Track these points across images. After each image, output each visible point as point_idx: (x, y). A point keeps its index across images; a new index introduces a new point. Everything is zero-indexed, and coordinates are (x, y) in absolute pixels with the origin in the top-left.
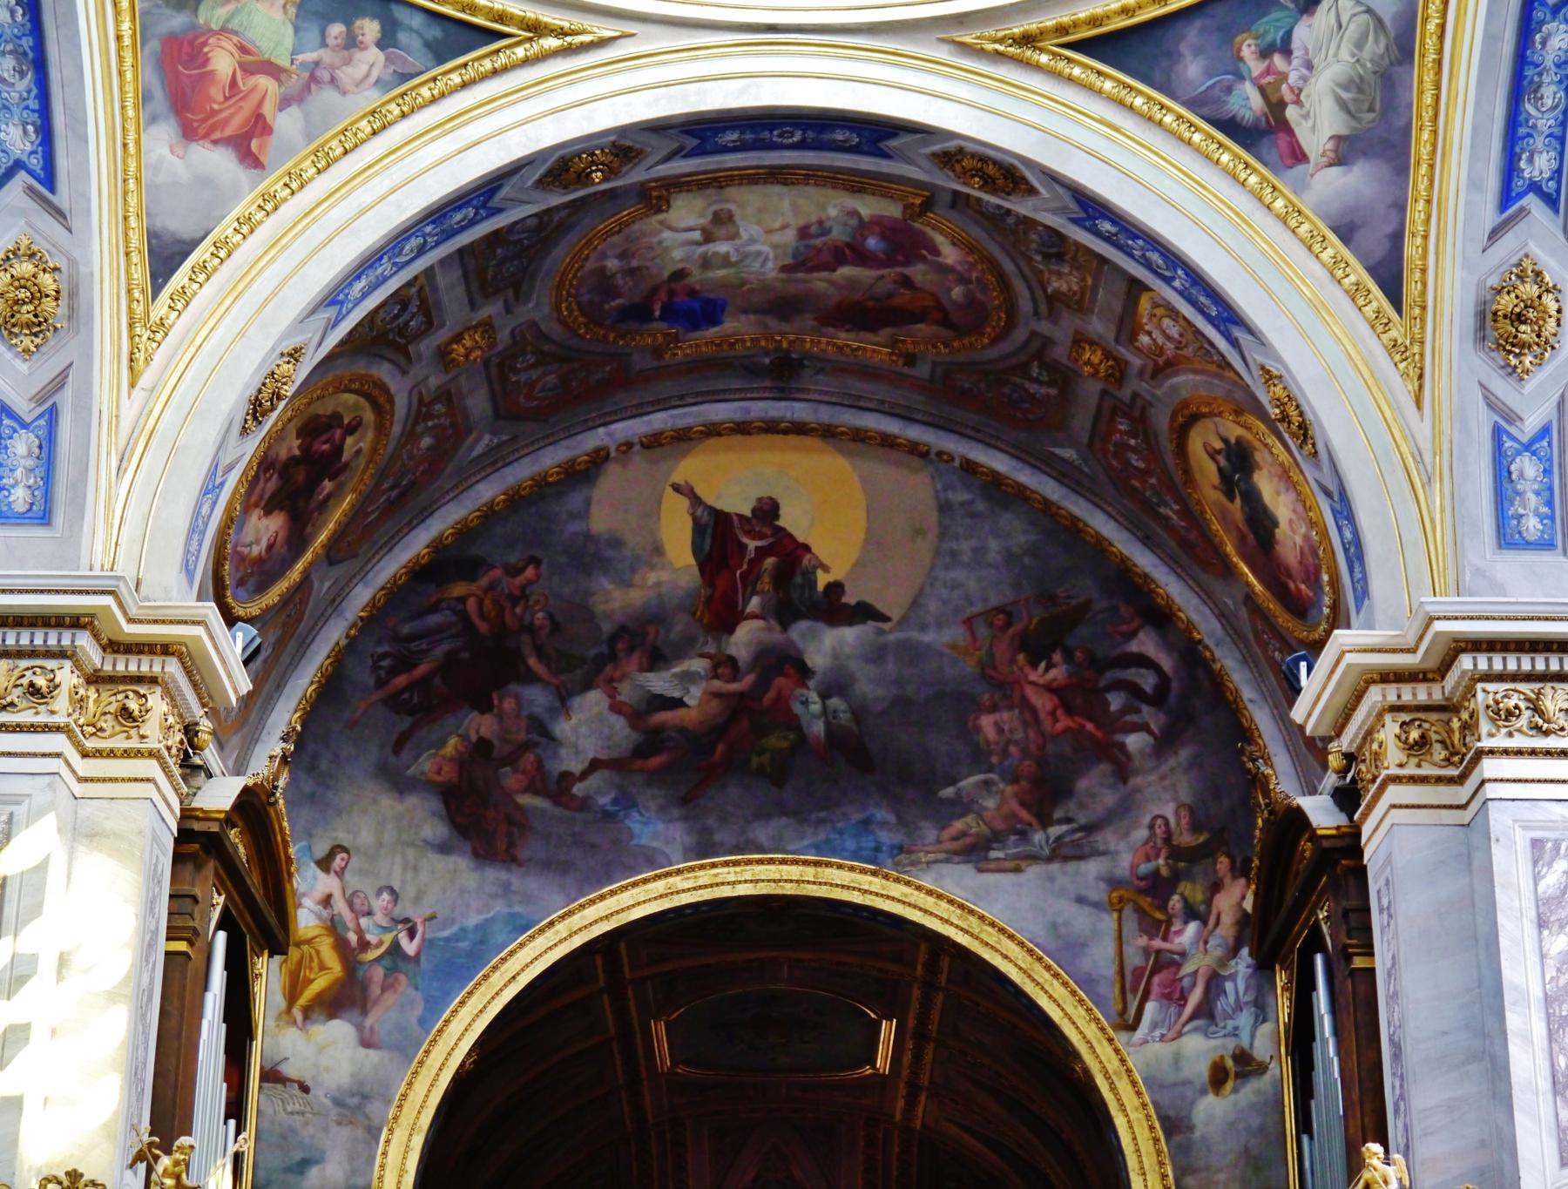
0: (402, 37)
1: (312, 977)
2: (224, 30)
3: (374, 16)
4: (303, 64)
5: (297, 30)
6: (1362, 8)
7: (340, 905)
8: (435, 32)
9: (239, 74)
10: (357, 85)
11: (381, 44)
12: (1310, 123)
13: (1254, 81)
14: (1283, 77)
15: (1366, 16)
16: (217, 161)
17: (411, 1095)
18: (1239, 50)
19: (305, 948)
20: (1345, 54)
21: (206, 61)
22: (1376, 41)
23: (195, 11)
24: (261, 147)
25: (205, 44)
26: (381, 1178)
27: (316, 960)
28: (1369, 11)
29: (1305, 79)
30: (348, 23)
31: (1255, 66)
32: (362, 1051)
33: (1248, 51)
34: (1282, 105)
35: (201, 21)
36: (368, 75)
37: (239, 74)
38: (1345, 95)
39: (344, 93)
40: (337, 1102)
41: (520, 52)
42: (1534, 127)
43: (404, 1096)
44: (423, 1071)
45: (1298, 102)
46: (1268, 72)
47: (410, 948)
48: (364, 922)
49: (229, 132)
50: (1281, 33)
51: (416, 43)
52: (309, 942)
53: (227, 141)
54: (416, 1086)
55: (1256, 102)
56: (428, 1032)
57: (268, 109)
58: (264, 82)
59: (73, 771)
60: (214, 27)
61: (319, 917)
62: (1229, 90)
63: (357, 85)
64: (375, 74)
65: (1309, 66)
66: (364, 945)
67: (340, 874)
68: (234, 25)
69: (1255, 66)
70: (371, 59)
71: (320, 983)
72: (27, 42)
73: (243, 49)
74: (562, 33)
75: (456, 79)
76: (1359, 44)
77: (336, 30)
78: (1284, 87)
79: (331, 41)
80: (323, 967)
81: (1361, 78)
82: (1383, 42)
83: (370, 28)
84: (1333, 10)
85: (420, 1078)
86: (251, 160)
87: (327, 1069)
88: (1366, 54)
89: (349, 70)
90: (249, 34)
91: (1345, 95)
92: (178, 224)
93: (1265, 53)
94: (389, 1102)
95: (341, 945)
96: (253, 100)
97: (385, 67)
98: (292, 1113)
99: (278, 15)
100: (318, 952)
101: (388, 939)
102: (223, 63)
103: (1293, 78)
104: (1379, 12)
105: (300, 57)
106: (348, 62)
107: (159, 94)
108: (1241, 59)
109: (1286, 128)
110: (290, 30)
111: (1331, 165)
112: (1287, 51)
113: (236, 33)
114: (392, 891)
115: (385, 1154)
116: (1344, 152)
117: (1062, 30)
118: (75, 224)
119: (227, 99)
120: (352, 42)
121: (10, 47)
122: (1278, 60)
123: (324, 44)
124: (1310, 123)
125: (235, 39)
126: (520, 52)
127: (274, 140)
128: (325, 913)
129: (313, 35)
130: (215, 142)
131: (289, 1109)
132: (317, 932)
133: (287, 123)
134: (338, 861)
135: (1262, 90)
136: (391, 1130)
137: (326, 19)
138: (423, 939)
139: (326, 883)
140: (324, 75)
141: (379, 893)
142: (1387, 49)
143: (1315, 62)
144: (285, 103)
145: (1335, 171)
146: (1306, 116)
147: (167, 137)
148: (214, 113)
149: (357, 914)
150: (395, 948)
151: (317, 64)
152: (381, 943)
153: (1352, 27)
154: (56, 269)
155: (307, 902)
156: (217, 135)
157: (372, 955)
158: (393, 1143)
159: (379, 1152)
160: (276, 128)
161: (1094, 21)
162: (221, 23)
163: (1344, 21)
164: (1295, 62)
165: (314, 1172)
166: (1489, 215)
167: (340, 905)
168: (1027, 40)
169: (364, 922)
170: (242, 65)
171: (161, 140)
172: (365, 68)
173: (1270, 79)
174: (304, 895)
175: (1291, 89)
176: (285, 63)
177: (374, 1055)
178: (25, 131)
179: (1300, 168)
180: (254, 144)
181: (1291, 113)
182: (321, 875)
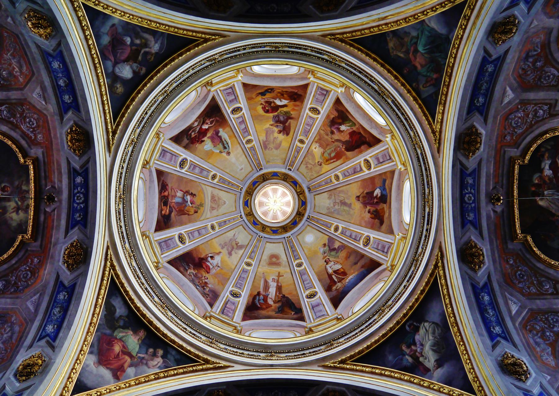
0: (169, 356)
2: (121, 340)
3: (162, 349)
4: (139, 357)
5: (140, 347)
6: (430, 324)
8: (178, 357)
9: (120, 353)
10: (153, 366)
11: (162, 357)
12: (427, 360)
13: (408, 355)
14: (416, 351)
15: (433, 325)
16: (106, 373)
18: (402, 348)
20: (431, 338)
21: (113, 346)
22: (438, 329)
23: (114, 332)
24: (120, 374)
25: (114, 341)
28: (433, 323)
29: (422, 349)
30: (155, 349)
31: (408, 351)
33: (404, 348)
34: (418, 358)
35: (115, 335)
36: (157, 365)
37: (120, 353)
38: (434, 348)
39: (149, 368)
41: (201, 367)
42: (490, 320)
45: (422, 356)
46: (411, 351)
49: (112, 367)
50: (411, 340)
51: (172, 358)
53: (111, 370)
55: (410, 359)
57: (126, 365)
58: (127, 357)
60: (118, 337)
62: (402, 359)
63: (153, 366)
64: (159, 365)
65: (422, 345)
68: (124, 339)
69: (408, 351)
70: (159, 361)
72: (65, 304)
73: (124, 347)
74: (213, 363)
75: (181, 371)
76: (434, 333)
77: (151, 350)
78: (417, 353)
79: (149, 353)
81: (437, 341)
82: (440, 330)
83: (160, 352)
84: (424, 328)
86: (117, 378)
88: (436, 334)
89: (152, 362)
90: (127, 343)
91: (434, 348)
92: (88, 382)
93: (409, 347)
96: (122, 361)
97: (162, 363)
99: (136, 341)
102: (117, 348)
103: (419, 350)
104: (436, 322)
105: (139, 355)
106: (152, 360)
107: (96, 347)
108: (403, 350)
109: (421, 364)
110: (138, 346)
111: (437, 369)
112: (415, 344)
113: (123, 342)
116: (439, 364)
117: (351, 357)
118: (56, 350)
119: (115, 358)
120: (154, 355)
121: (60, 305)
122: (413, 347)
123: (146, 353)
124: (427, 360)
125: (122, 343)
126: (201, 367)
127: (125, 374)
129: (144, 350)
130: (107, 368)
133: (131, 371)
135: (411, 356)
137: (149, 346)
140: (145, 362)
142: (442, 330)
143: (424, 343)
144: (131, 366)
145: (439, 369)
146: (426, 359)
147: (94, 359)
148: (110, 360)
151: (143, 358)
153: (430, 329)
154: (44, 361)
156: (108, 366)
160: (126, 371)
161: (359, 353)
162: (120, 337)
163: (427, 329)
164: (418, 346)
166: (489, 343)
168: (343, 362)
170: (122, 351)
171: (90, 360)
172: (156, 363)
173: (412, 353)
175: (419, 353)
176: (134, 354)
178: (54, 327)
179: (429, 373)
180: (119, 373)
181: (421, 359)
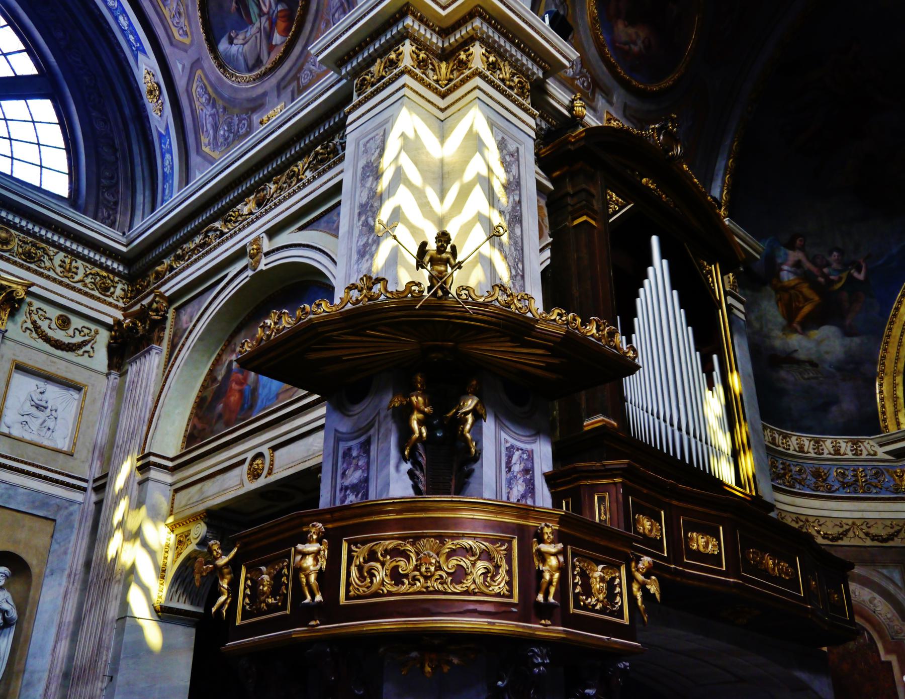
1: (801, 305)
7: (808, 265)
17: (888, 356)
19: (792, 292)
26: (883, 406)
27: (801, 296)
32: (847, 340)
40: (839, 368)
43: (884, 357)
44: (892, 340)
47: (861, 276)
48: (826, 270)
52: (794, 287)
54: (890, 350)
56: (887, 319)
59: (412, 89)
61: (795, 273)
66: (831, 282)
67: (802, 249)
71: (807, 309)
80: (807, 300)
85: (890, 344)
87: (827, 353)
94: (875, 364)
95: (815, 286)
98: (808, 379)
100: (801, 292)
101: (844, 275)
114: (838, 250)
115: (881, 392)
128: (799, 271)
131: (806, 376)
132: (796, 282)
134: (798, 242)
136: (882, 378)
138: (867, 269)
139: (794, 256)
141: (830, 254)
149: (820, 268)
150: (851, 279)
152: (840, 279)
155: (785, 267)
157: (838, 286)
158: (885, 385)
159: (877, 391)
165: (834, 409)
167: (808, 265)
169: (826, 270)
174: (782, 264)
177: (856, 340)
182: (790, 252)
